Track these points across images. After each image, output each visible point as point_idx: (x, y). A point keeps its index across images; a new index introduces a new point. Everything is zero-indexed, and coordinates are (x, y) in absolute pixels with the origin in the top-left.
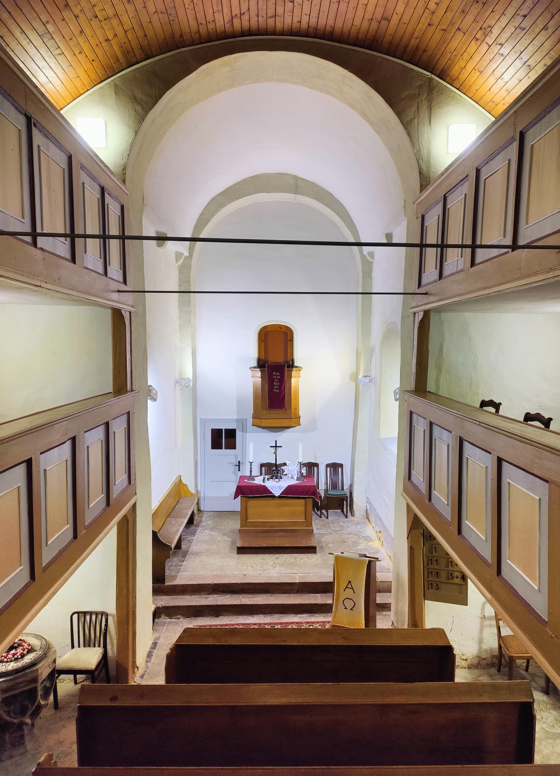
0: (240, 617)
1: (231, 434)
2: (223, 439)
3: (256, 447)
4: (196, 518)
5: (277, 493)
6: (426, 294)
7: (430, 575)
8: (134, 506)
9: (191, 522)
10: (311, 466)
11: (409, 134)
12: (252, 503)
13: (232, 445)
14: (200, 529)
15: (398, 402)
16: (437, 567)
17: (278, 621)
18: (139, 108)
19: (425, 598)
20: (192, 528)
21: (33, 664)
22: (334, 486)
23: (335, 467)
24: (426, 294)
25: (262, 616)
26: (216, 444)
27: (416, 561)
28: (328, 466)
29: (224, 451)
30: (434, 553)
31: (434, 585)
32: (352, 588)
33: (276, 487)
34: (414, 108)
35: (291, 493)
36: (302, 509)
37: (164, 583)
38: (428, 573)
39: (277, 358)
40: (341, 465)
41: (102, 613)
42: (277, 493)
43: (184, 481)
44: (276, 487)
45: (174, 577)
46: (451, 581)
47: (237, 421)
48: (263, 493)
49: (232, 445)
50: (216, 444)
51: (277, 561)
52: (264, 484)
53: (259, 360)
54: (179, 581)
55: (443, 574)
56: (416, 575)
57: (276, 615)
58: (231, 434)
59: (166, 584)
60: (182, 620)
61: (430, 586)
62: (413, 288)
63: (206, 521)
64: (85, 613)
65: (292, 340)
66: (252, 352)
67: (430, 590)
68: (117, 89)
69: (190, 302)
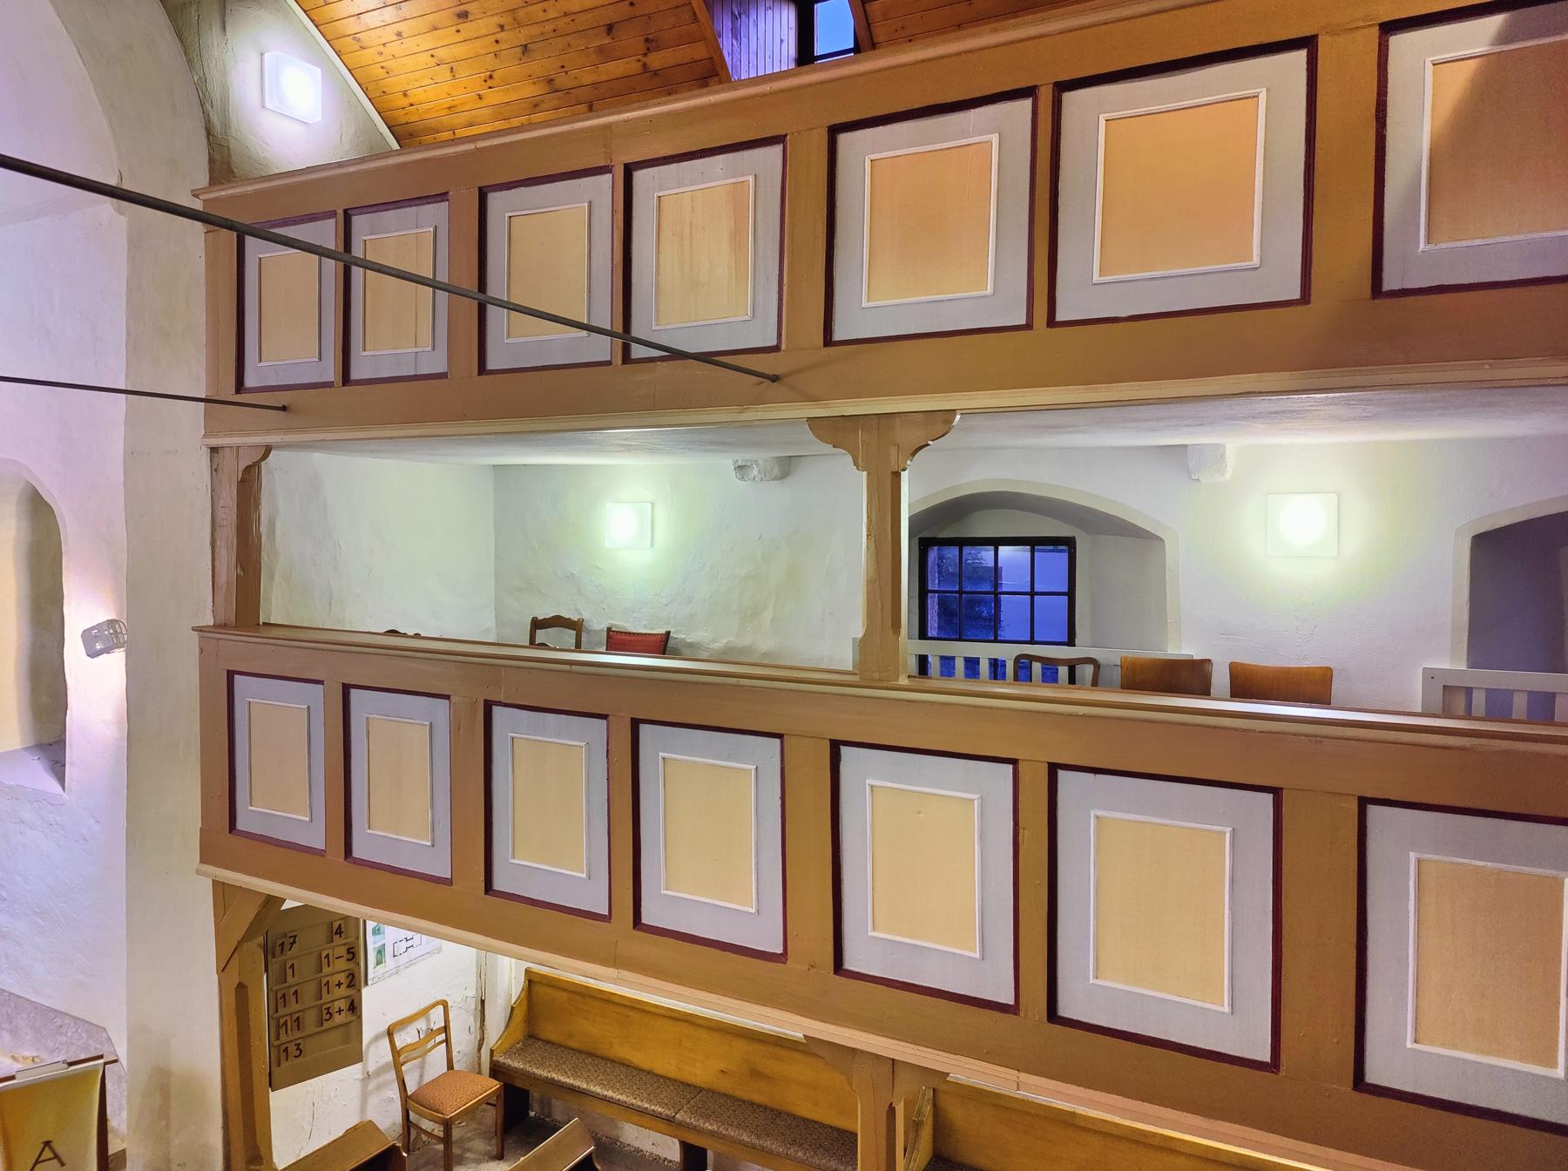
6: (284, 408)
7: (282, 1031)
15: (117, 659)
16: (294, 1007)
19: (273, 1085)
24: (284, 408)
27: (252, 1014)
30: (290, 980)
31: (292, 1049)
32: (56, 1156)
38: (278, 1027)
46: (327, 1025)
55: (310, 1018)
56: (255, 1043)
61: (283, 1055)
62: (229, 393)
67: (284, 1064)
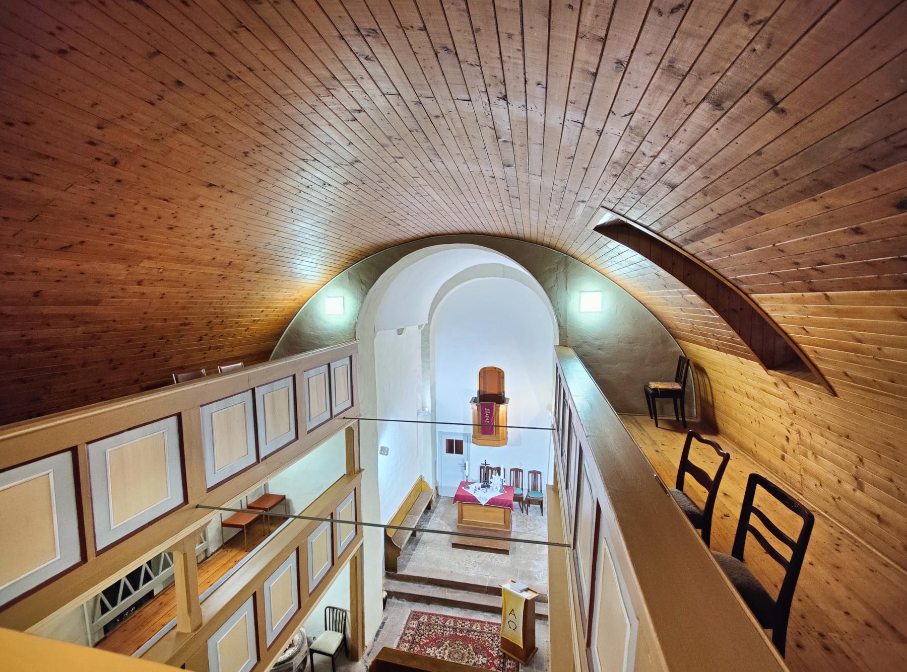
0: (444, 608)
1: (459, 444)
2: (455, 447)
3: (478, 454)
4: (434, 503)
5: (484, 503)
8: (362, 545)
9: (428, 508)
10: (517, 471)
11: (550, 298)
12: (466, 507)
13: (460, 451)
14: (434, 515)
17: (469, 617)
18: (364, 287)
20: (429, 514)
21: (291, 658)
22: (535, 488)
23: (535, 473)
25: (459, 609)
26: (450, 450)
28: (530, 472)
29: (454, 455)
33: (484, 496)
34: (554, 278)
35: (493, 502)
36: (502, 515)
37: (396, 571)
39: (492, 390)
40: (540, 473)
41: (343, 611)
42: (484, 503)
43: (426, 480)
44: (484, 496)
45: (404, 566)
47: (464, 435)
48: (473, 501)
49: (460, 451)
50: (450, 450)
51: (479, 560)
52: (474, 494)
53: (479, 392)
54: (406, 572)
57: (469, 611)
58: (459, 444)
59: (398, 573)
60: (405, 602)
63: (440, 509)
64: (333, 608)
65: (503, 378)
66: (474, 390)
68: (350, 276)
69: (429, 355)
